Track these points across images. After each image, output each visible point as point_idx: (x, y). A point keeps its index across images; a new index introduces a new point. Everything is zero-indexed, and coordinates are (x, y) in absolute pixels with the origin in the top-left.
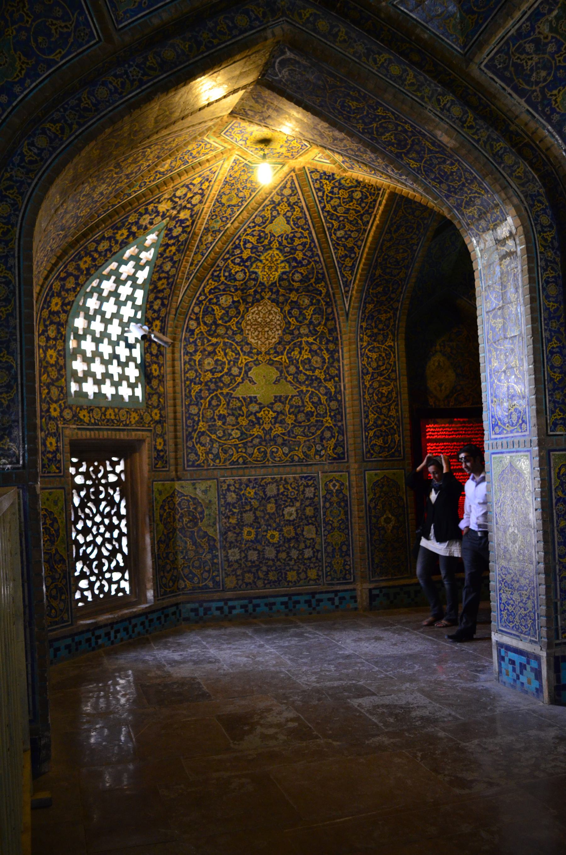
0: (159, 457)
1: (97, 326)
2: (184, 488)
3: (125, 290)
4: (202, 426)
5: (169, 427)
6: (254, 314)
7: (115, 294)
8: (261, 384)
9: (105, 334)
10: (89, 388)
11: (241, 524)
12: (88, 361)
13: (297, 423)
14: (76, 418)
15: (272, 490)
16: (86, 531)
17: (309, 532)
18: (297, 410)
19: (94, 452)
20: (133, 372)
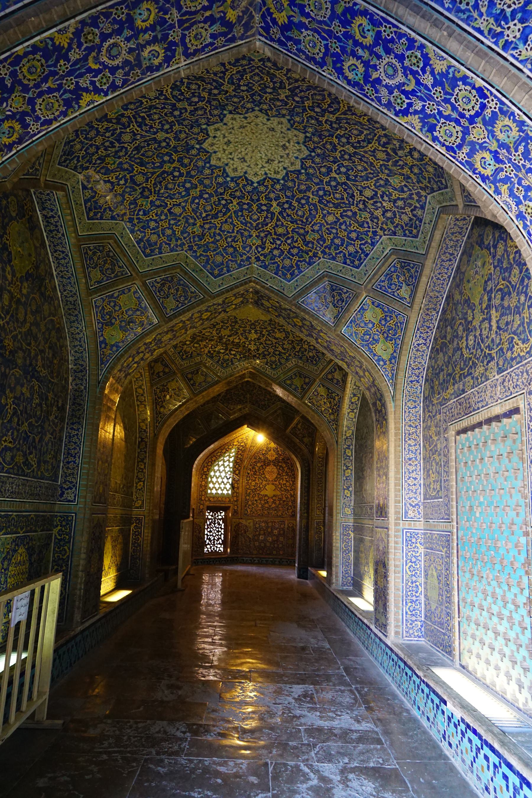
0: (235, 512)
1: (218, 474)
2: (243, 522)
3: (226, 464)
4: (250, 503)
5: (239, 503)
6: (268, 469)
7: (223, 465)
8: (269, 490)
9: (220, 476)
10: (214, 491)
11: (259, 535)
12: (214, 484)
13: (280, 504)
14: (209, 500)
15: (270, 524)
16: (210, 532)
17: (281, 539)
18: (280, 499)
19: (215, 509)
20: (228, 486)
